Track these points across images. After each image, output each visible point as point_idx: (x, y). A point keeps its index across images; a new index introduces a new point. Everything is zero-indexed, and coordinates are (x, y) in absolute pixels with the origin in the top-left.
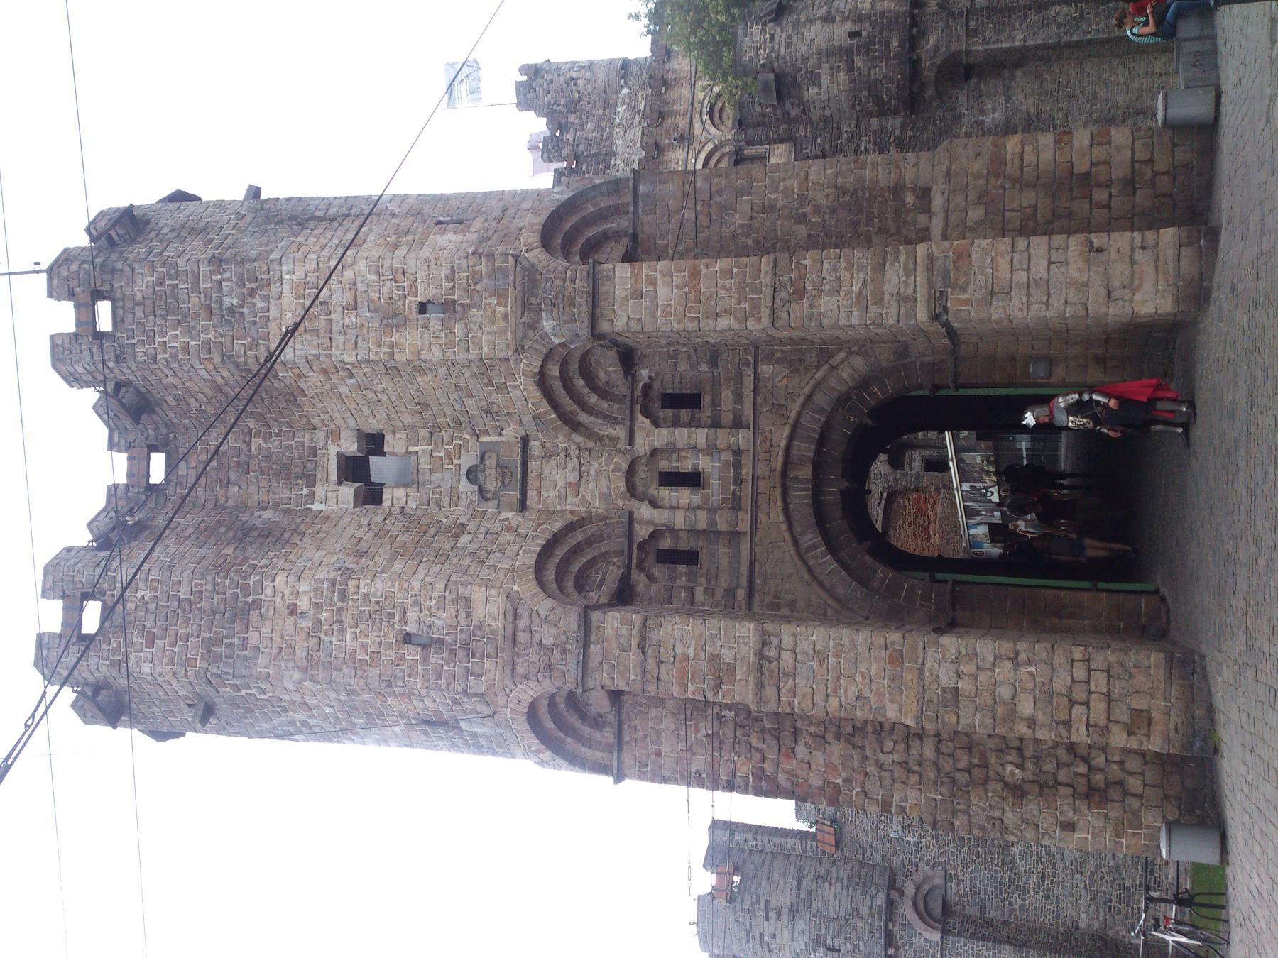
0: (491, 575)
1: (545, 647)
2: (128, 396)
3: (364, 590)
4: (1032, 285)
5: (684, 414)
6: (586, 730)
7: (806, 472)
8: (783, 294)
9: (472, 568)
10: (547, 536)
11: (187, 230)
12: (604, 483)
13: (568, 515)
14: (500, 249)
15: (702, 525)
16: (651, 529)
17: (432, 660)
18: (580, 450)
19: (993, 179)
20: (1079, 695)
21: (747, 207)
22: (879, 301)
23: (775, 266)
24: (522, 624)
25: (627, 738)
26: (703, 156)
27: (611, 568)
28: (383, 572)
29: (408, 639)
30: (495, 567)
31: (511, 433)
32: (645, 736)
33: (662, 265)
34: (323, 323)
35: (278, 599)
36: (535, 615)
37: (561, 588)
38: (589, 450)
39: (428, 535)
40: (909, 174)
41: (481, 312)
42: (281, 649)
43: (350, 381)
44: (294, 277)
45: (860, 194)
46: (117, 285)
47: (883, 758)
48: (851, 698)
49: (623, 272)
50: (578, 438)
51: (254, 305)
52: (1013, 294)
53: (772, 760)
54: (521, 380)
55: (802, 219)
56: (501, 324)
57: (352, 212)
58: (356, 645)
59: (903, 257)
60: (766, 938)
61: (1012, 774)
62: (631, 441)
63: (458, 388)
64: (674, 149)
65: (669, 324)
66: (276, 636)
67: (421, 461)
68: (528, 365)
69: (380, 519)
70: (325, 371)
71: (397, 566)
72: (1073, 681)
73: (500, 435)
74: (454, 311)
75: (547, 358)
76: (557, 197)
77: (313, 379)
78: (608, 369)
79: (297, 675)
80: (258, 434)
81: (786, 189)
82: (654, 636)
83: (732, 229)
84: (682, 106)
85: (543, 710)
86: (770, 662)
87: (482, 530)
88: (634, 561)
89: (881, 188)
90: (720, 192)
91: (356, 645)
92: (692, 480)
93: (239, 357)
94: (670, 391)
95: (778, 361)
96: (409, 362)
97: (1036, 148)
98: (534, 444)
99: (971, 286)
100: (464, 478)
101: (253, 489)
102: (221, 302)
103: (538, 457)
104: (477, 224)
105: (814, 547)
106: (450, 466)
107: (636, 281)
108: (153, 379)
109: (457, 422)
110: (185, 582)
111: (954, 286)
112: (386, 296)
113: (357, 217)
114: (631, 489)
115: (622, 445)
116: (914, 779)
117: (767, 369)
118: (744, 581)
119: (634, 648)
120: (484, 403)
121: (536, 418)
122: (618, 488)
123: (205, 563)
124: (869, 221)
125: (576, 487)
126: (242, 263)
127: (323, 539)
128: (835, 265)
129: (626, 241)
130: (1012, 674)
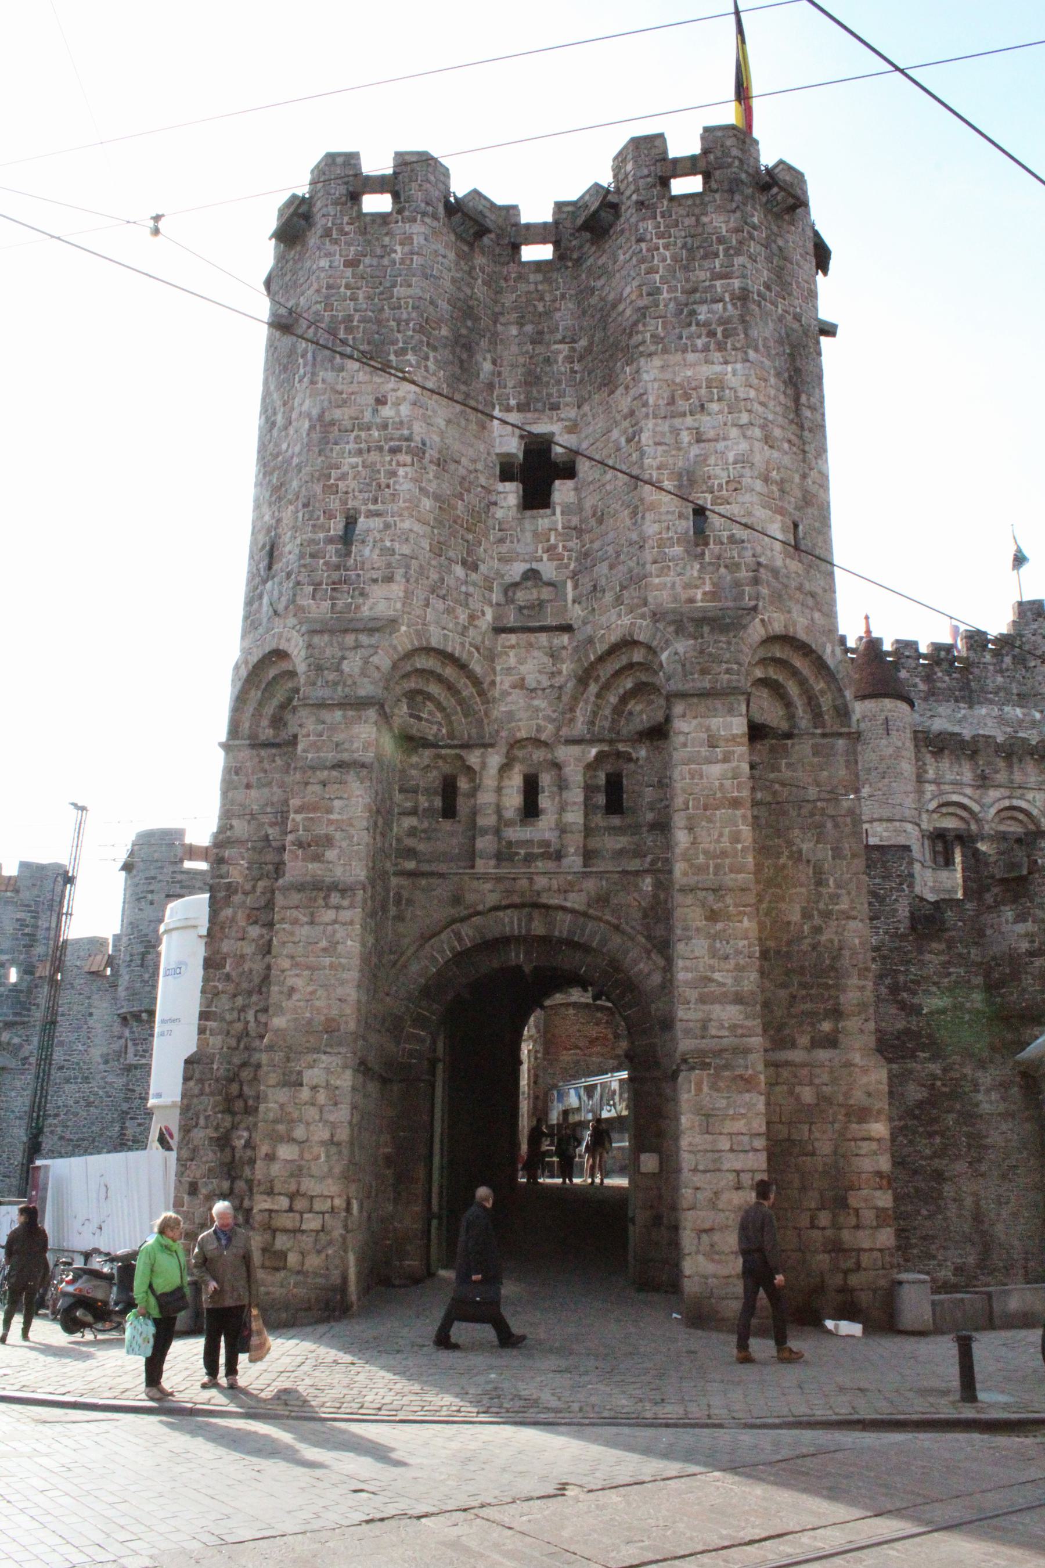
0: (417, 602)
1: (340, 663)
2: (606, 216)
3: (401, 472)
4: (716, 1155)
5: (601, 799)
7: (538, 928)
8: (711, 898)
9: (426, 582)
10: (465, 656)
11: (781, 263)
12: (523, 715)
13: (488, 680)
14: (765, 591)
15: (482, 821)
16: (477, 768)
17: (329, 547)
18: (560, 688)
19: (843, 1111)
21: (820, 855)
22: (702, 1000)
23: (742, 890)
24: (364, 639)
25: (263, 753)
26: (965, 801)
27: (435, 727)
28: (421, 489)
29: (351, 522)
30: (427, 605)
31: (576, 613)
32: (266, 771)
33: (745, 767)
34: (681, 409)
36: (372, 651)
37: (406, 676)
38: (559, 698)
39: (465, 533)
40: (852, 1024)
41: (696, 574)
42: (341, 393)
43: (623, 440)
44: (729, 376)
45: (832, 974)
46: (717, 196)
48: (291, 982)
49: (738, 726)
51: (699, 337)
52: (706, 1136)
53: (244, 902)
54: (626, 620)
55: (806, 915)
56: (684, 596)
57: (806, 433)
58: (345, 468)
59: (749, 1023)
60: (150, 896)
61: (240, 1137)
63: (618, 554)
64: (974, 771)
65: (681, 776)
66: (354, 387)
67: (546, 520)
68: (640, 628)
69: (483, 481)
70: (632, 413)
71: (427, 503)
72: (312, 1197)
73: (574, 601)
74: (697, 545)
75: (649, 648)
76: (829, 650)
77: (623, 401)
79: (315, 412)
80: (573, 349)
81: (838, 896)
82: (351, 777)
83: (798, 841)
84: (1018, 777)
85: (284, 666)
86: (324, 898)
87: (471, 589)
88: (443, 751)
89: (838, 997)
90: (836, 826)
91: (345, 468)
92: (531, 810)
93: (644, 325)
94: (625, 782)
95: (655, 896)
96: (642, 500)
97: (875, 1153)
98: (565, 638)
99: (715, 1094)
100: (527, 566)
101: (514, 349)
102: (703, 302)
103: (551, 643)
104: (794, 566)
105: (460, 939)
106: (540, 551)
107: (727, 740)
108: (622, 240)
109: (586, 555)
110: (410, 291)
111: (717, 1076)
112: (712, 472)
113: (801, 437)
114: (516, 744)
115: (565, 732)
116: (233, 1042)
117: (647, 884)
118: (425, 867)
119: (339, 756)
121: (590, 641)
122: (519, 730)
123: (431, 309)
124: (803, 985)
125: (520, 684)
126: (743, 321)
127: (458, 425)
128: (741, 953)
129: (784, 726)
130: (316, 1138)
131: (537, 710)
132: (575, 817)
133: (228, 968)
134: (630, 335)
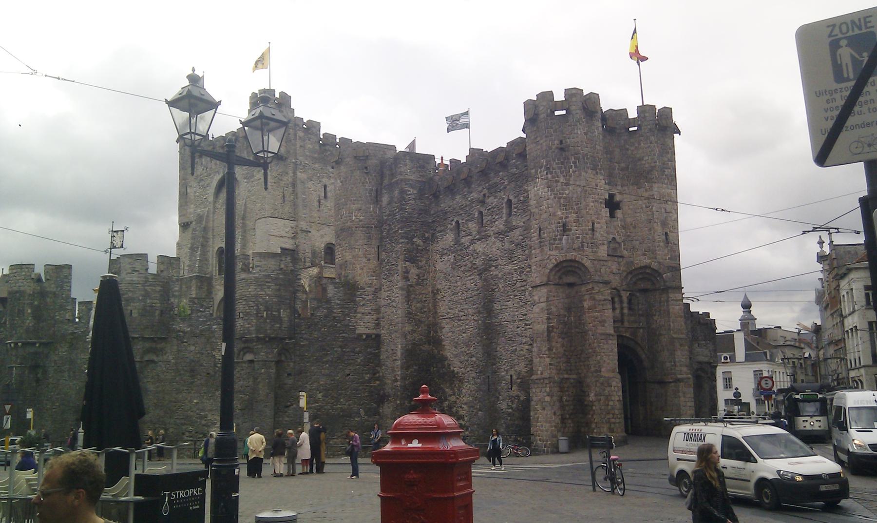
6: (559, 274)
20: (615, 416)
22: (681, 366)
25: (557, 287)
29: (593, 224)
31: (625, 253)
35: (599, 181)
43: (644, 206)
47: (561, 364)
50: (625, 274)
58: (590, 207)
62: (624, 290)
66: (591, 180)
73: (624, 249)
78: (642, 285)
80: (619, 166)
91: (590, 207)
98: (621, 260)
100: (612, 236)
102: (666, 168)
109: (629, 236)
120: (637, 247)
131: (616, 280)
132: (626, 311)
133: (554, 351)
134: (648, 173)
